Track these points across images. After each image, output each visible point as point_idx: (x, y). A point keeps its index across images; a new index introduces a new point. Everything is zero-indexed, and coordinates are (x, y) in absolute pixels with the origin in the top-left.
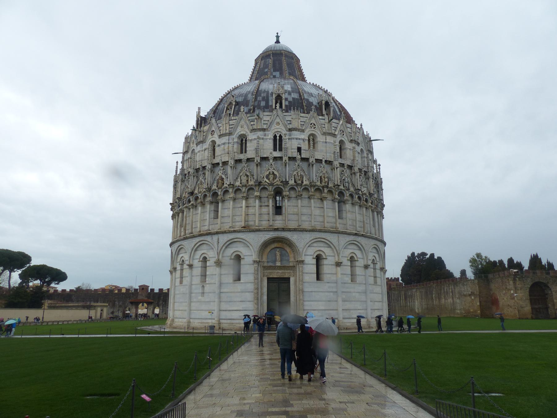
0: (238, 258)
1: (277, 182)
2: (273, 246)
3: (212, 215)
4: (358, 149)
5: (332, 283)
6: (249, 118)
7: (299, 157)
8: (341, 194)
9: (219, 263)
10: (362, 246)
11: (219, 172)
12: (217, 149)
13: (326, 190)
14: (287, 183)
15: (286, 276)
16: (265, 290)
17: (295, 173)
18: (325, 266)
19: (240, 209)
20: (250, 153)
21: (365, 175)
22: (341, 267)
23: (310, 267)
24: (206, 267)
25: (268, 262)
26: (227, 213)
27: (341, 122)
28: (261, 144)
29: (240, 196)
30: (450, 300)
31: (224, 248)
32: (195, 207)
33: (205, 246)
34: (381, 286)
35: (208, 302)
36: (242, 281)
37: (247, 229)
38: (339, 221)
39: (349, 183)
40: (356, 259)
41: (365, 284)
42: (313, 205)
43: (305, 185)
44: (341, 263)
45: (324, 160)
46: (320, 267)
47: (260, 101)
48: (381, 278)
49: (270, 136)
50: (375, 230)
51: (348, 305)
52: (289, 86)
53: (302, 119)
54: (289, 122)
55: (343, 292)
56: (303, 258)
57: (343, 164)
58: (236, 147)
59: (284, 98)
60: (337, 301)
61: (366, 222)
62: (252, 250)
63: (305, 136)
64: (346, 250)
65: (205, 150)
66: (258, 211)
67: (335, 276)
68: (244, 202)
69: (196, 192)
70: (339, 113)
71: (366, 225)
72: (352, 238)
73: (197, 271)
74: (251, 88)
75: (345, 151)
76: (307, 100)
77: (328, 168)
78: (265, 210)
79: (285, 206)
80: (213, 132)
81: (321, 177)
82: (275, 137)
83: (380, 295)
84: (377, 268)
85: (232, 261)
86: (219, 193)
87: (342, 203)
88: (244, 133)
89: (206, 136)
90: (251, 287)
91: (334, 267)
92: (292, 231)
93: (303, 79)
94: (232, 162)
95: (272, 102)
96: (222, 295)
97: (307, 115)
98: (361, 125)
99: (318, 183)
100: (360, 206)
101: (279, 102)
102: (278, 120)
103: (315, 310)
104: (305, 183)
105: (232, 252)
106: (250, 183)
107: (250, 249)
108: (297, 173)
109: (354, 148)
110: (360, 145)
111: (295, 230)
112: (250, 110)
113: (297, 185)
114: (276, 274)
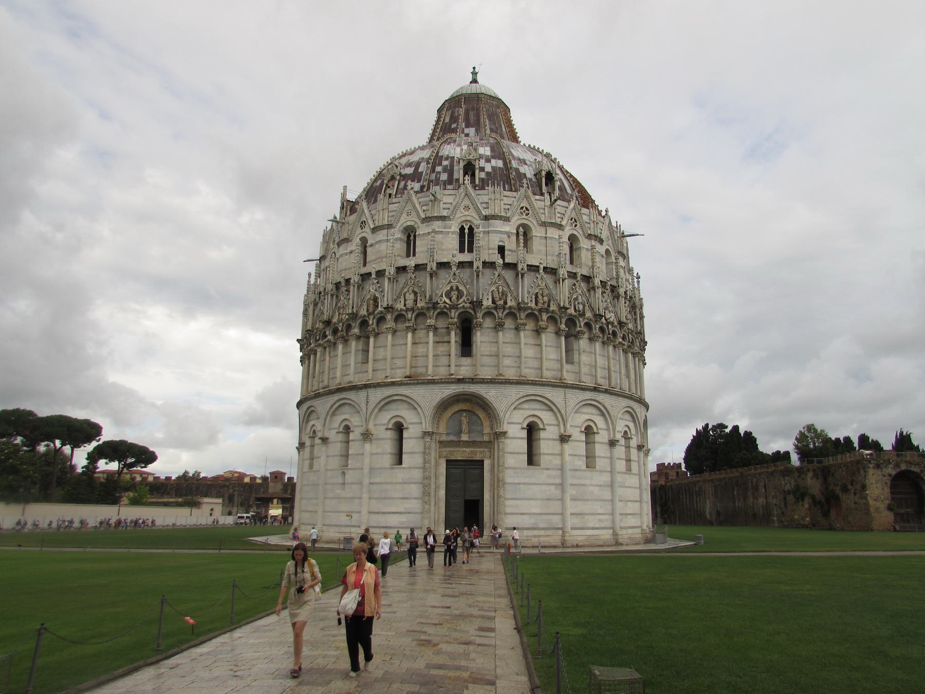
1: (463, 303)
2: (456, 408)
3: (360, 356)
4: (601, 249)
5: (554, 469)
6: (420, 200)
7: (501, 261)
8: (571, 322)
10: (606, 408)
11: (371, 288)
12: (369, 250)
13: (545, 316)
14: (479, 303)
15: (478, 457)
16: (442, 480)
17: (494, 288)
19: (403, 347)
20: (420, 258)
21: (612, 291)
22: (570, 443)
23: (516, 442)
24: (348, 442)
25: (447, 434)
26: (381, 353)
27: (572, 205)
29: (401, 326)
30: (761, 501)
31: (376, 410)
33: (347, 407)
34: (639, 475)
35: (351, 498)
36: (403, 465)
37: (413, 380)
38: (567, 367)
39: (584, 306)
40: (595, 430)
41: (611, 472)
42: (523, 340)
43: (510, 308)
44: (570, 436)
45: (542, 267)
46: (534, 443)
47: (439, 173)
48: (639, 462)
49: (455, 228)
50: (629, 383)
51: (580, 507)
52: (488, 149)
53: (506, 200)
54: (485, 205)
55: (572, 485)
56: (505, 427)
57: (575, 274)
58: (400, 247)
59: (477, 166)
60: (562, 500)
61: (613, 369)
63: (511, 228)
64: (578, 415)
67: (559, 457)
68: (410, 335)
69: (335, 320)
70: (569, 191)
71: (613, 375)
72: (588, 395)
73: (336, 448)
74: (426, 154)
75: (578, 252)
76: (517, 170)
77: (549, 279)
78: (442, 348)
81: (536, 295)
82: (462, 229)
83: (638, 491)
84: (631, 445)
85: (389, 432)
86: (371, 322)
87: (573, 338)
88: (412, 223)
89: (352, 231)
90: (417, 474)
91: (558, 443)
92: (488, 383)
93: (514, 138)
95: (458, 173)
96: (374, 487)
97: (515, 194)
99: (533, 305)
100: (603, 343)
101: (470, 173)
103: (524, 514)
104: (509, 304)
105: (389, 417)
106: (419, 305)
107: (419, 412)
108: (498, 288)
109: (593, 247)
110: (605, 243)
111: (492, 382)
112: (422, 187)
114: (461, 454)
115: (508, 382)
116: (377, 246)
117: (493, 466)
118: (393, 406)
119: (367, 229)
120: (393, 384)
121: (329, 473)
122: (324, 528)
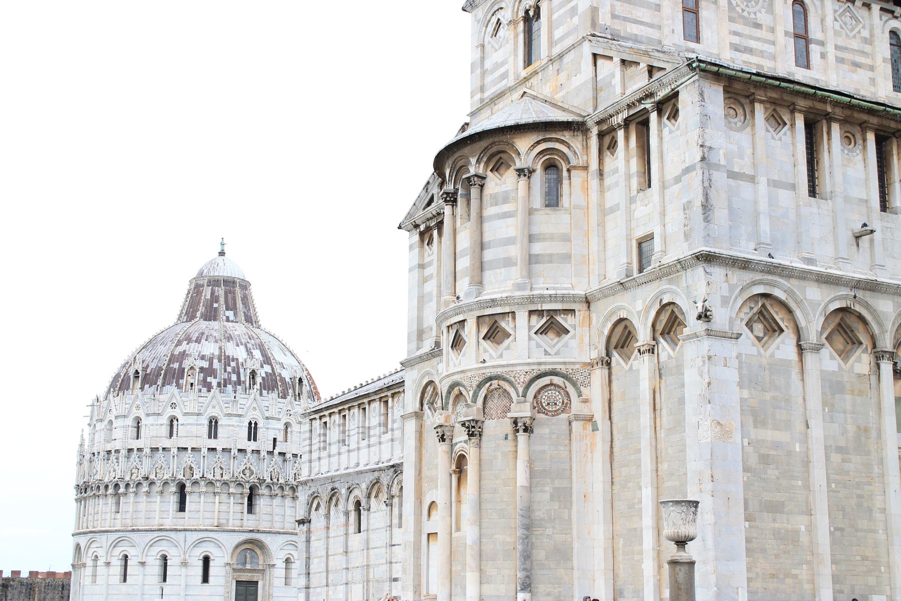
0: (206, 560)
1: (253, 480)
2: (244, 547)
9: (184, 564)
15: (255, 580)
29: (211, 489)
32: (148, 493)
33: (164, 542)
37: (220, 528)
53: (280, 405)
66: (231, 509)
82: (250, 423)
89: (164, 410)
94: (204, 451)
102: (255, 405)
111: (269, 532)
113: (273, 484)
114: (245, 577)
115: (279, 533)
117: (264, 586)
118: (204, 544)
120: (206, 530)
121: (146, 587)
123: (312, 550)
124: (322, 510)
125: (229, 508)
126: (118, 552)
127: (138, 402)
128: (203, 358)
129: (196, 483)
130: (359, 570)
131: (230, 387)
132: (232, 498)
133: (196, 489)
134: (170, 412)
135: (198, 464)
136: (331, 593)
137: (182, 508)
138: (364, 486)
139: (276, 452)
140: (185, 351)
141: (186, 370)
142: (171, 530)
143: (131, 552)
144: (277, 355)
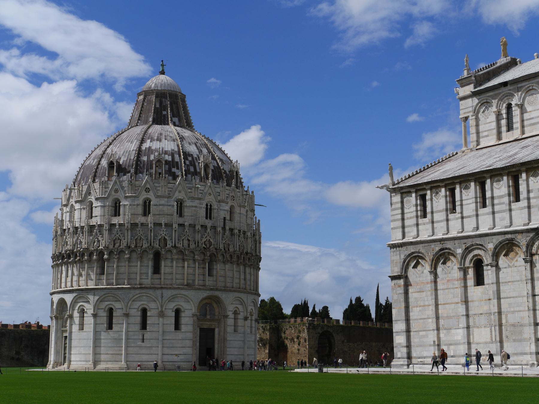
6: (187, 185)
8: (249, 259)
9: (162, 314)
15: (213, 327)
16: (198, 338)
18: (239, 320)
26: (168, 270)
28: (195, 212)
29: (181, 257)
33: (145, 297)
42: (235, 269)
49: (204, 206)
53: (227, 192)
62: (193, 305)
65: (138, 205)
79: (217, 269)
80: (147, 190)
82: (207, 205)
88: (182, 198)
89: (140, 193)
91: (243, 320)
94: (175, 226)
96: (165, 341)
98: (253, 192)
102: (210, 191)
105: (174, 305)
114: (206, 325)
115: (230, 291)
116: (161, 207)
119: (151, 193)
120: (179, 288)
121: (130, 333)
122: (128, 363)
123: (411, 300)
124: (426, 268)
125: (195, 271)
126: (104, 305)
127: (116, 187)
128: (166, 153)
129: (170, 251)
130: (483, 317)
131: (189, 176)
132: (197, 264)
133: (169, 256)
134: (144, 196)
135: (171, 236)
136: (442, 335)
137: (157, 270)
138: (491, 246)
139: (227, 228)
140: (150, 147)
141: (154, 162)
142: (150, 288)
143: (117, 305)
144: (217, 154)
